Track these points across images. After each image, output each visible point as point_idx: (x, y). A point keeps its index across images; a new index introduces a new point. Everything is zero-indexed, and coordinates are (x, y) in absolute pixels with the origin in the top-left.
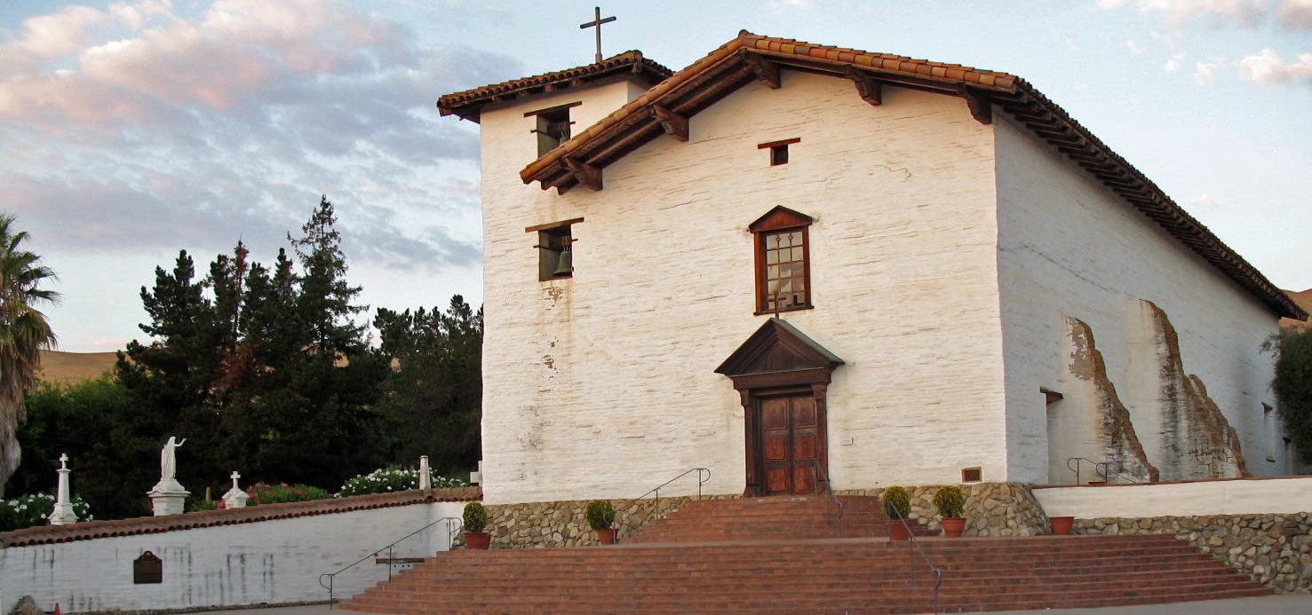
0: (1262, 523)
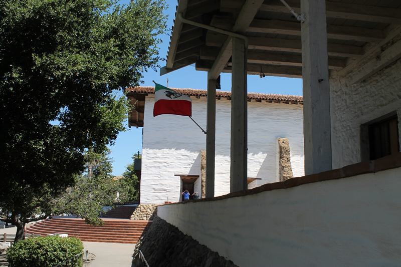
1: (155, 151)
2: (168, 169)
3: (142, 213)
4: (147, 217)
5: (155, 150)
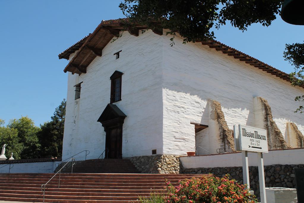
1: (173, 93)
3: (169, 166)
4: (175, 170)
5: (174, 92)
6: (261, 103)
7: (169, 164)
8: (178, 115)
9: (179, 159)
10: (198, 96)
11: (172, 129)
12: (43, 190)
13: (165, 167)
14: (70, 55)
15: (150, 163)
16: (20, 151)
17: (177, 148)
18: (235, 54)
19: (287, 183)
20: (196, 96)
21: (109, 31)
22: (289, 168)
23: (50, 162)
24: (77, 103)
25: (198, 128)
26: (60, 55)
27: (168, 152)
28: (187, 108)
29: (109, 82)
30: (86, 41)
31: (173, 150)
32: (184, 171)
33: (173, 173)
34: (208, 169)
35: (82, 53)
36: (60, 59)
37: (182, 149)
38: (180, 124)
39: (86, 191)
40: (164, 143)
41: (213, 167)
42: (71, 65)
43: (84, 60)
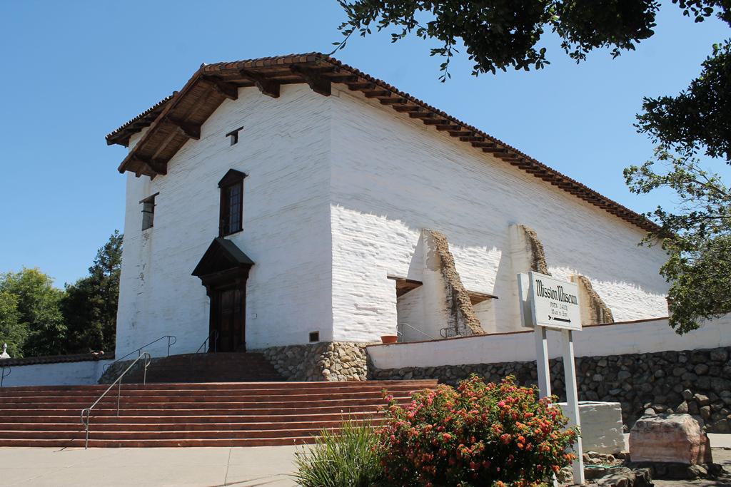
0: (505, 370)
1: (353, 215)
2: (378, 262)
3: (346, 365)
4: (358, 373)
5: (354, 213)
6: (524, 236)
7: (347, 361)
8: (363, 261)
9: (365, 350)
10: (402, 221)
11: (350, 289)
12: (85, 421)
13: (338, 367)
14: (132, 136)
15: (306, 360)
16: (21, 341)
17: (360, 329)
18: (475, 139)
19: (587, 393)
20: (398, 222)
21: (215, 86)
22: (590, 362)
23: (89, 362)
24: (147, 237)
25: (401, 287)
26: (109, 136)
27: (344, 336)
28: (381, 247)
29: (217, 194)
30: (168, 108)
31: (352, 333)
32: (375, 374)
33: (354, 379)
34: (427, 369)
35: (159, 132)
36: (108, 144)
37: (371, 330)
38: (367, 279)
39: (177, 420)
40: (334, 318)
41: (436, 365)
42: (135, 157)
43: (163, 147)
